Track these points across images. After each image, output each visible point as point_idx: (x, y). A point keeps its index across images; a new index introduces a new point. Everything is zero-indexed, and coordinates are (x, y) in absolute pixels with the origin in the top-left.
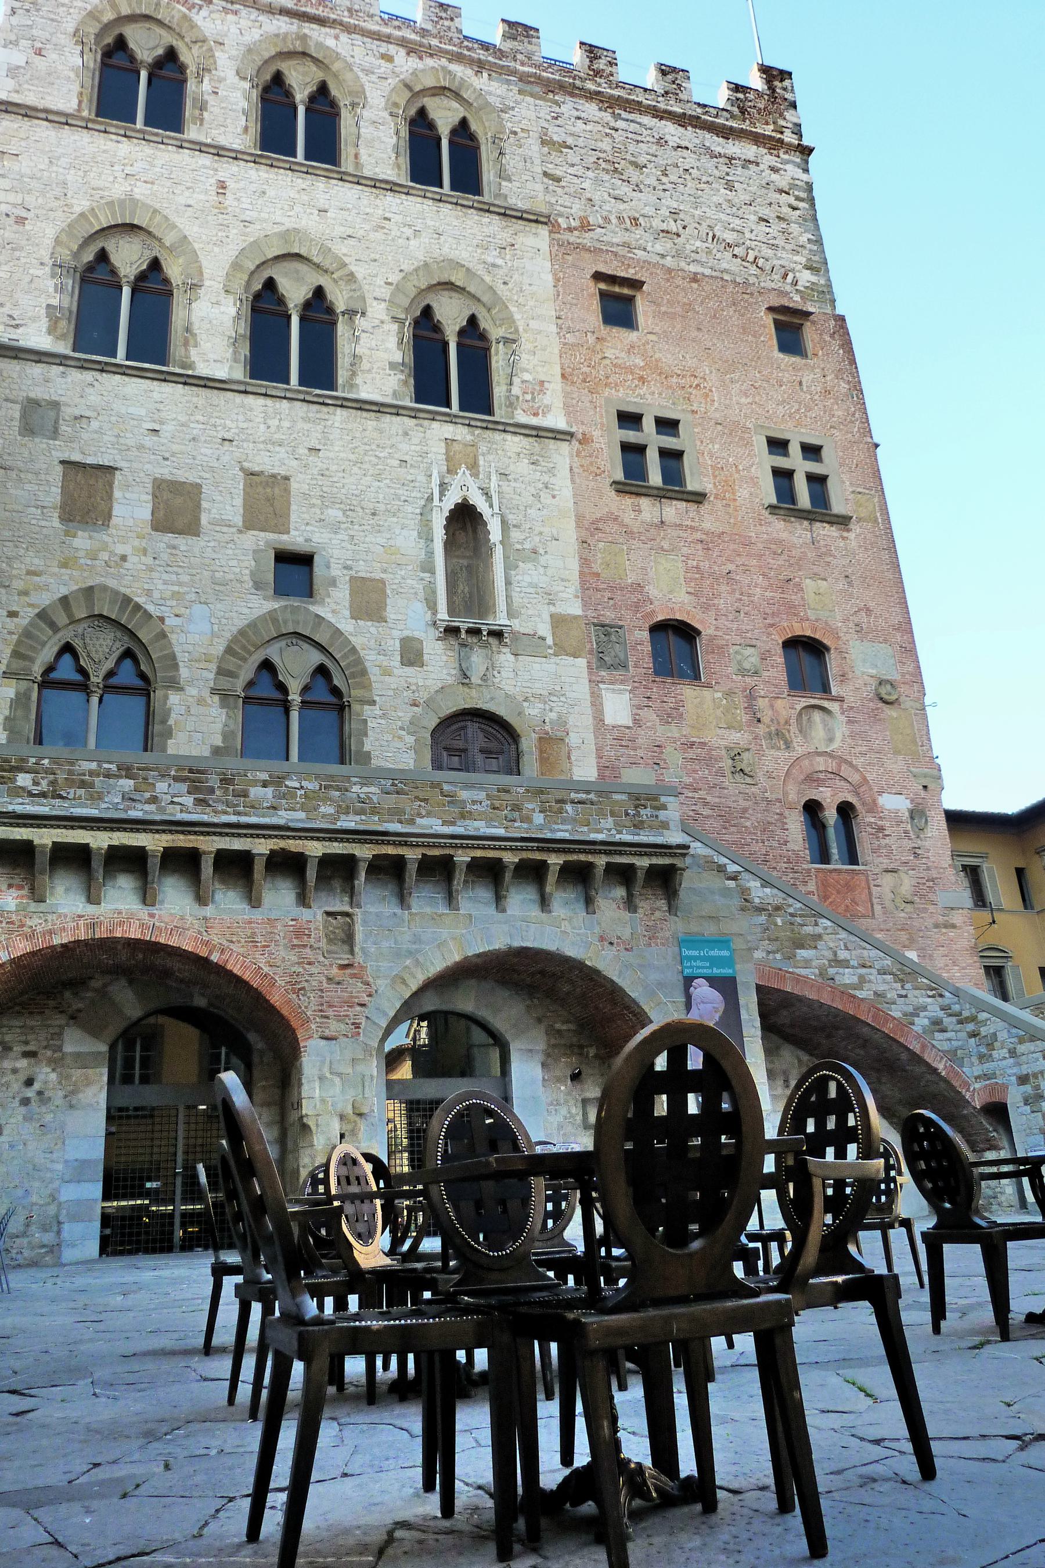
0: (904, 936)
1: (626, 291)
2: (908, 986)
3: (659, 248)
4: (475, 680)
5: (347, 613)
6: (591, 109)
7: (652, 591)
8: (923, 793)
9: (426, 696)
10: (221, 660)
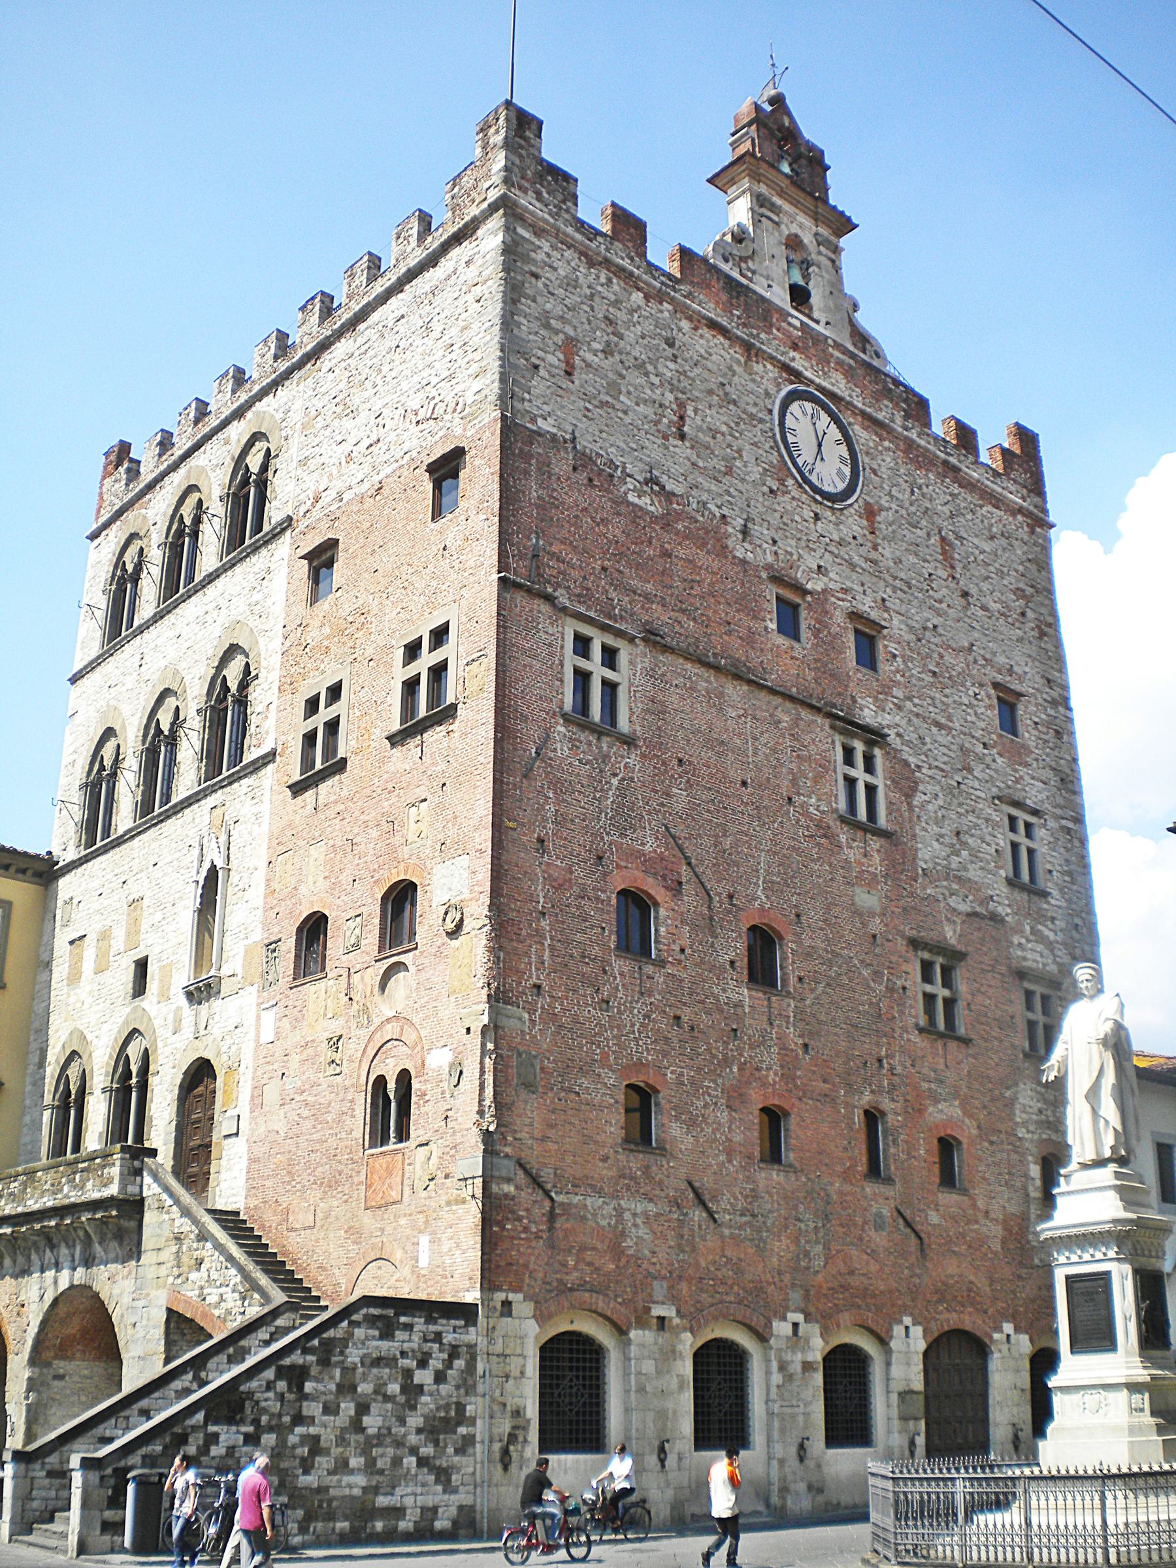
0: (421, 1219)
1: (329, 554)
2: (246, 1303)
4: (202, 1032)
5: (155, 1000)
6: (342, 347)
7: (303, 890)
9: (178, 1056)
10: (108, 1064)
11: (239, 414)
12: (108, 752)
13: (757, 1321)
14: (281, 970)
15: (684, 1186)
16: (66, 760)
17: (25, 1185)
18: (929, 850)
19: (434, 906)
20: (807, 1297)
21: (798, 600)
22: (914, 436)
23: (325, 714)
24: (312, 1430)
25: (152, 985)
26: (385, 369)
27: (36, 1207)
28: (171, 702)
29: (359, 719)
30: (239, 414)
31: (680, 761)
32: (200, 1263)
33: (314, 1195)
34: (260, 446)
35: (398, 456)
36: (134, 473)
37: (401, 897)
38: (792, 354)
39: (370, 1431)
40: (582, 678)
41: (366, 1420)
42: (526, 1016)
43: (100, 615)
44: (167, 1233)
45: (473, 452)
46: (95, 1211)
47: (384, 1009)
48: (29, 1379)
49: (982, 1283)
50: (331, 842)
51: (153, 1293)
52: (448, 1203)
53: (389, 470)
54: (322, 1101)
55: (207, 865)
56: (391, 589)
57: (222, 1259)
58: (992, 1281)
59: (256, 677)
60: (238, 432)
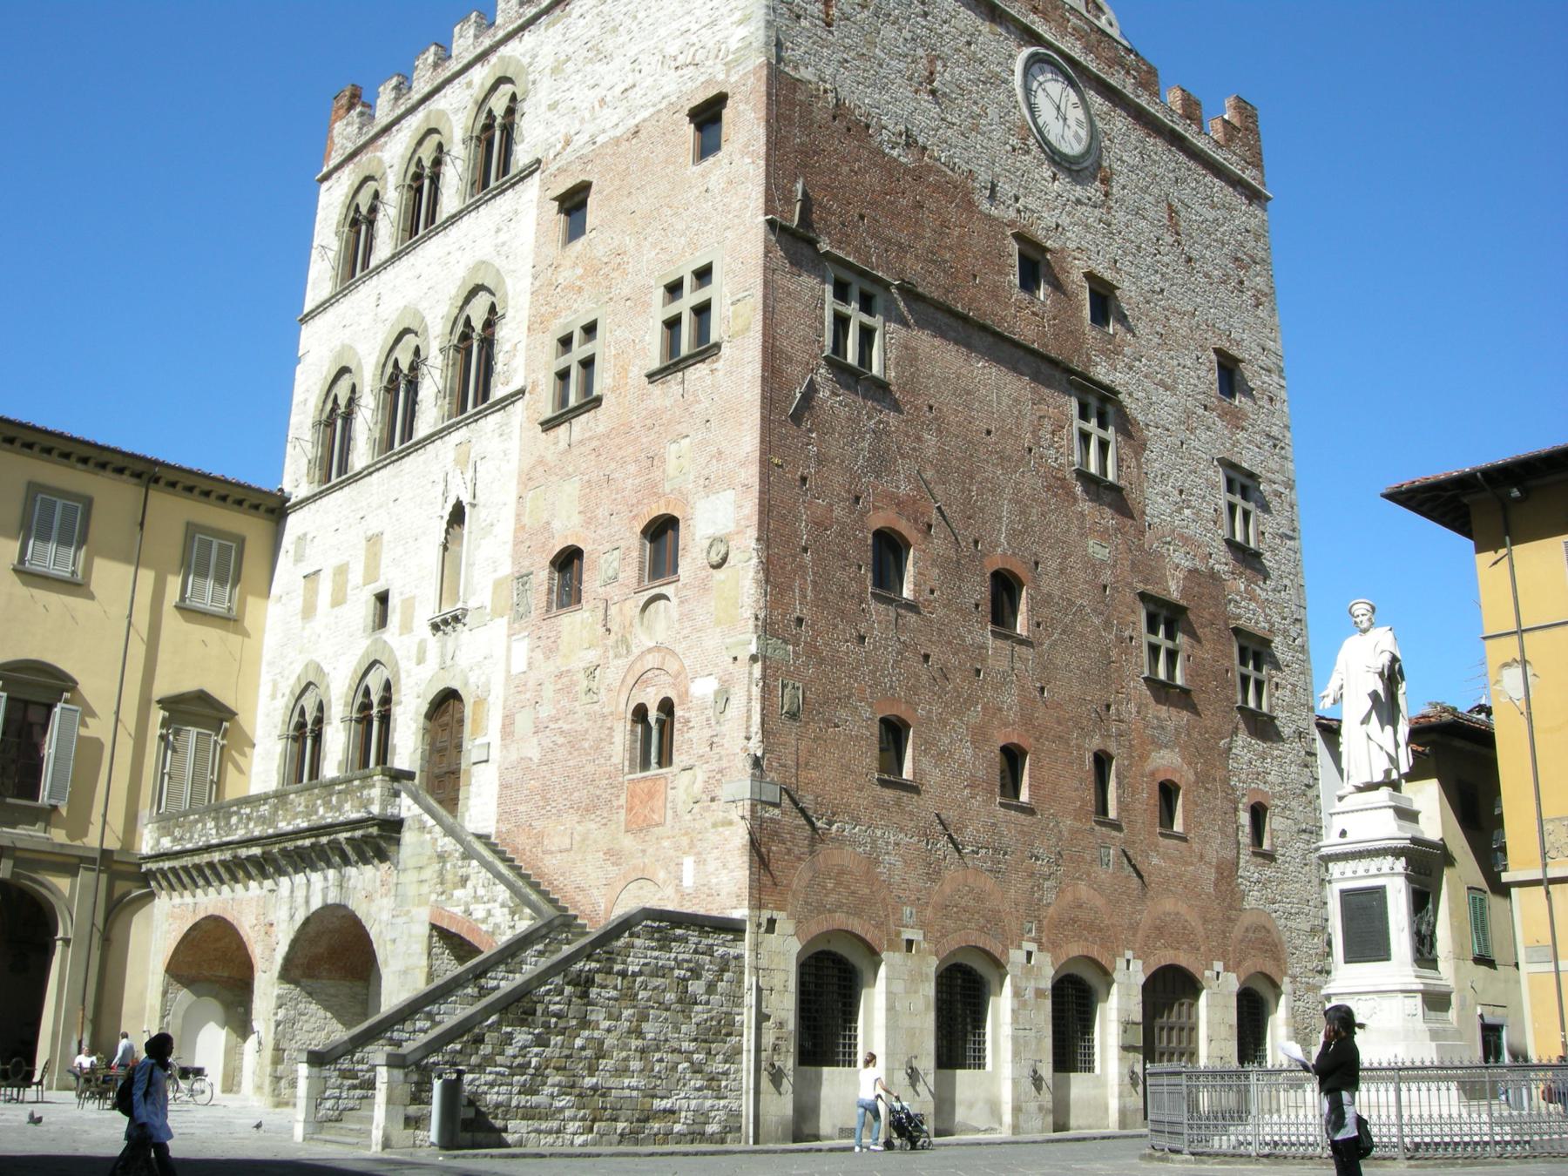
0: (685, 841)
3: (615, 120)
4: (449, 662)
7: (556, 525)
8: (731, 667)
9: (423, 686)
11: (482, 57)
12: (342, 390)
13: (995, 948)
14: (533, 602)
15: (933, 817)
16: (298, 396)
17: (276, 808)
18: (1157, 505)
19: (697, 538)
20: (1039, 930)
21: (1039, 257)
22: (1144, 104)
23: (579, 351)
24: (596, 1034)
25: (394, 618)
26: (641, 15)
27: (290, 828)
28: (410, 341)
29: (617, 356)
30: (482, 57)
31: (931, 408)
32: (464, 881)
33: (571, 819)
34: (506, 89)
35: (657, 100)
36: (368, 116)
37: (662, 531)
38: (1032, 16)
39: (649, 1036)
40: (841, 322)
41: (645, 1027)
42: (790, 648)
43: (331, 254)
44: (429, 851)
45: (738, 97)
46: (354, 829)
47: (642, 640)
48: (279, 997)
49: (1193, 920)
50: (586, 478)
51: (414, 910)
52: (715, 825)
53: (645, 114)
54: (579, 728)
55: (452, 502)
56: (649, 230)
57: (489, 875)
58: (1205, 921)
59: (503, 316)
60: (481, 76)
